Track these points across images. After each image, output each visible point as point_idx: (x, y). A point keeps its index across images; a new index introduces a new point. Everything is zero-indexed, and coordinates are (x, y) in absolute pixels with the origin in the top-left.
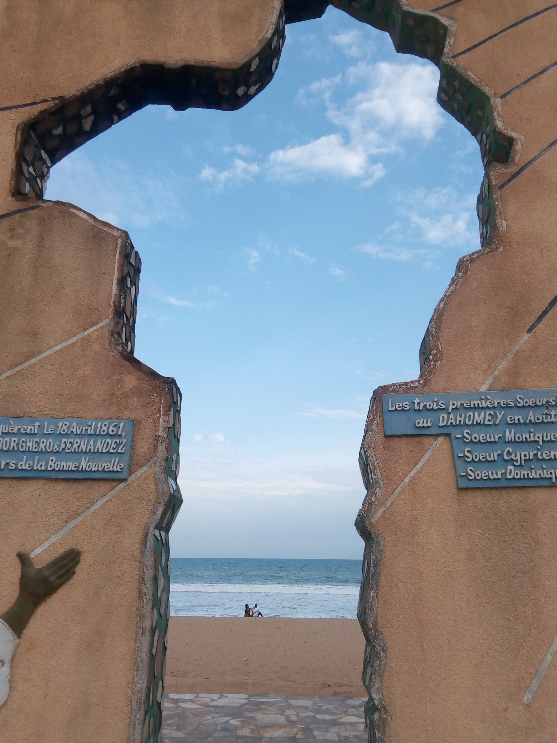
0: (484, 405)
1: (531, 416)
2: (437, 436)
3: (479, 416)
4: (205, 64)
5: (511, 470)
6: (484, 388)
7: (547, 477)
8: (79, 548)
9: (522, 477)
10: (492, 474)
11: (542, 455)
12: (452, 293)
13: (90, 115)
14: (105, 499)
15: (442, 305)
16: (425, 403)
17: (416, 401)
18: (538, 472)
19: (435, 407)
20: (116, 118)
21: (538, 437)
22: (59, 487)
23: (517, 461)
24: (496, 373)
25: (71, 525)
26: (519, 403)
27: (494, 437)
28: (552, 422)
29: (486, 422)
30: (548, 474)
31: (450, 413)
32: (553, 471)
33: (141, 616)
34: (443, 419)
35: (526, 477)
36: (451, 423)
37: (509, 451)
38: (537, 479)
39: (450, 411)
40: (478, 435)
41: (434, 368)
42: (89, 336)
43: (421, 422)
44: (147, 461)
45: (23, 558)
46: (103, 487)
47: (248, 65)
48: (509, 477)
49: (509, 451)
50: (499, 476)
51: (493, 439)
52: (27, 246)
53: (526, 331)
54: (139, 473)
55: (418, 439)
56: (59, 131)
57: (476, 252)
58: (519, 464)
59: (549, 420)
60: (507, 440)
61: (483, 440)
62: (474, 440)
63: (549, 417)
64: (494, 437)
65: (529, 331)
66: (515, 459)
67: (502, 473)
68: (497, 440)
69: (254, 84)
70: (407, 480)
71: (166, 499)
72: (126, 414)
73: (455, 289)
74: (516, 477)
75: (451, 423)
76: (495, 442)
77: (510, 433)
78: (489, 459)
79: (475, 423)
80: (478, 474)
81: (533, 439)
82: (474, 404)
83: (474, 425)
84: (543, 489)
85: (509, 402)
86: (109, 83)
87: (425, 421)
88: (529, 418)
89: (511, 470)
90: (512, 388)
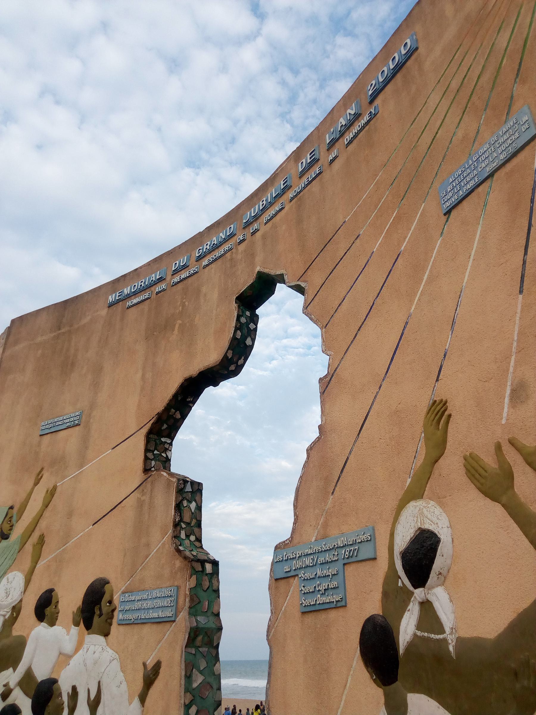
2: (294, 576)
4: (207, 367)
6: (313, 540)
8: (162, 660)
13: (175, 412)
14: (170, 631)
20: (191, 405)
22: (155, 626)
25: (158, 647)
33: (180, 696)
42: (165, 541)
44: (182, 609)
45: (144, 665)
46: (168, 625)
47: (225, 356)
52: (146, 498)
54: (180, 616)
55: (287, 579)
56: (165, 426)
65: (333, 493)
69: (240, 359)
70: (283, 609)
71: (189, 630)
72: (176, 584)
86: (175, 396)
90: (325, 537)
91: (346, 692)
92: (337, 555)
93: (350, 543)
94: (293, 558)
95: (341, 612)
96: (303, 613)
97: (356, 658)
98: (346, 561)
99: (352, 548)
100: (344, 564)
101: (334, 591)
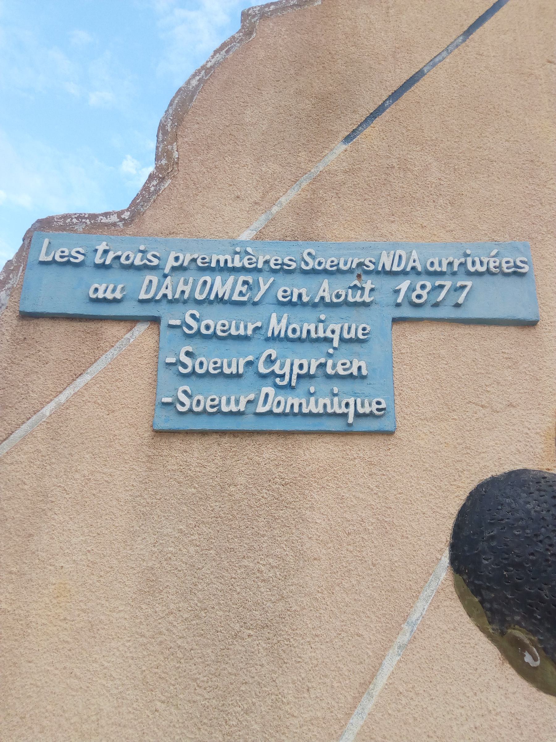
0: (238, 264)
1: (326, 289)
2: (134, 320)
3: (223, 285)
5: (267, 395)
6: (246, 235)
7: (339, 411)
9: (288, 410)
10: (228, 402)
11: (334, 366)
12: (218, 63)
15: (194, 83)
16: (119, 253)
17: (101, 248)
18: (321, 402)
19: (138, 262)
21: (333, 332)
23: (282, 376)
24: (275, 209)
26: (307, 264)
27: (246, 328)
28: (364, 304)
29: (236, 297)
30: (340, 406)
31: (165, 276)
32: (351, 401)
34: (147, 286)
35: (296, 410)
36: (165, 296)
37: (270, 356)
38: (318, 415)
39: (167, 271)
40: (215, 321)
41: (156, 191)
43: (102, 289)
48: (261, 409)
49: (270, 356)
50: (242, 407)
51: (242, 332)
53: (341, 138)
55: (92, 326)
57: (272, 4)
58: (285, 382)
59: (358, 299)
60: (270, 334)
61: (224, 331)
62: (204, 331)
63: (359, 292)
64: (246, 328)
65: (348, 139)
66: (281, 372)
67: (249, 402)
68: (249, 332)
70: (47, 410)
73: (225, 59)
74: (276, 410)
75: (165, 296)
76: (246, 338)
77: (279, 321)
78: (227, 371)
79: (212, 297)
80: (199, 402)
81: (321, 334)
82: (218, 261)
83: (211, 302)
84: (328, 439)
85: (286, 261)
87: (111, 287)
88: (321, 293)
89: (267, 395)
91: (368, 705)
92: (372, 290)
93: (437, 268)
94: (145, 267)
95: (363, 448)
96: (160, 433)
97: (429, 592)
98: (407, 312)
99: (448, 284)
100: (396, 321)
101: (348, 386)
